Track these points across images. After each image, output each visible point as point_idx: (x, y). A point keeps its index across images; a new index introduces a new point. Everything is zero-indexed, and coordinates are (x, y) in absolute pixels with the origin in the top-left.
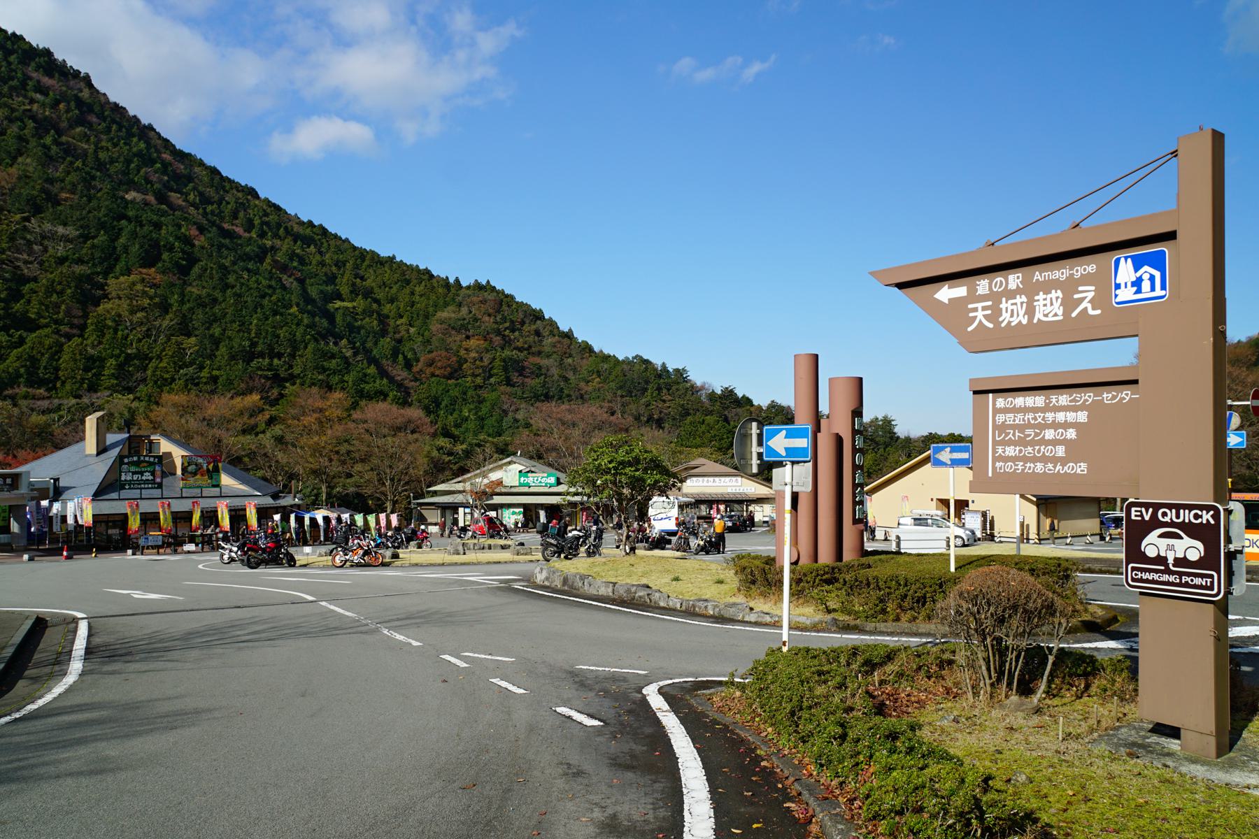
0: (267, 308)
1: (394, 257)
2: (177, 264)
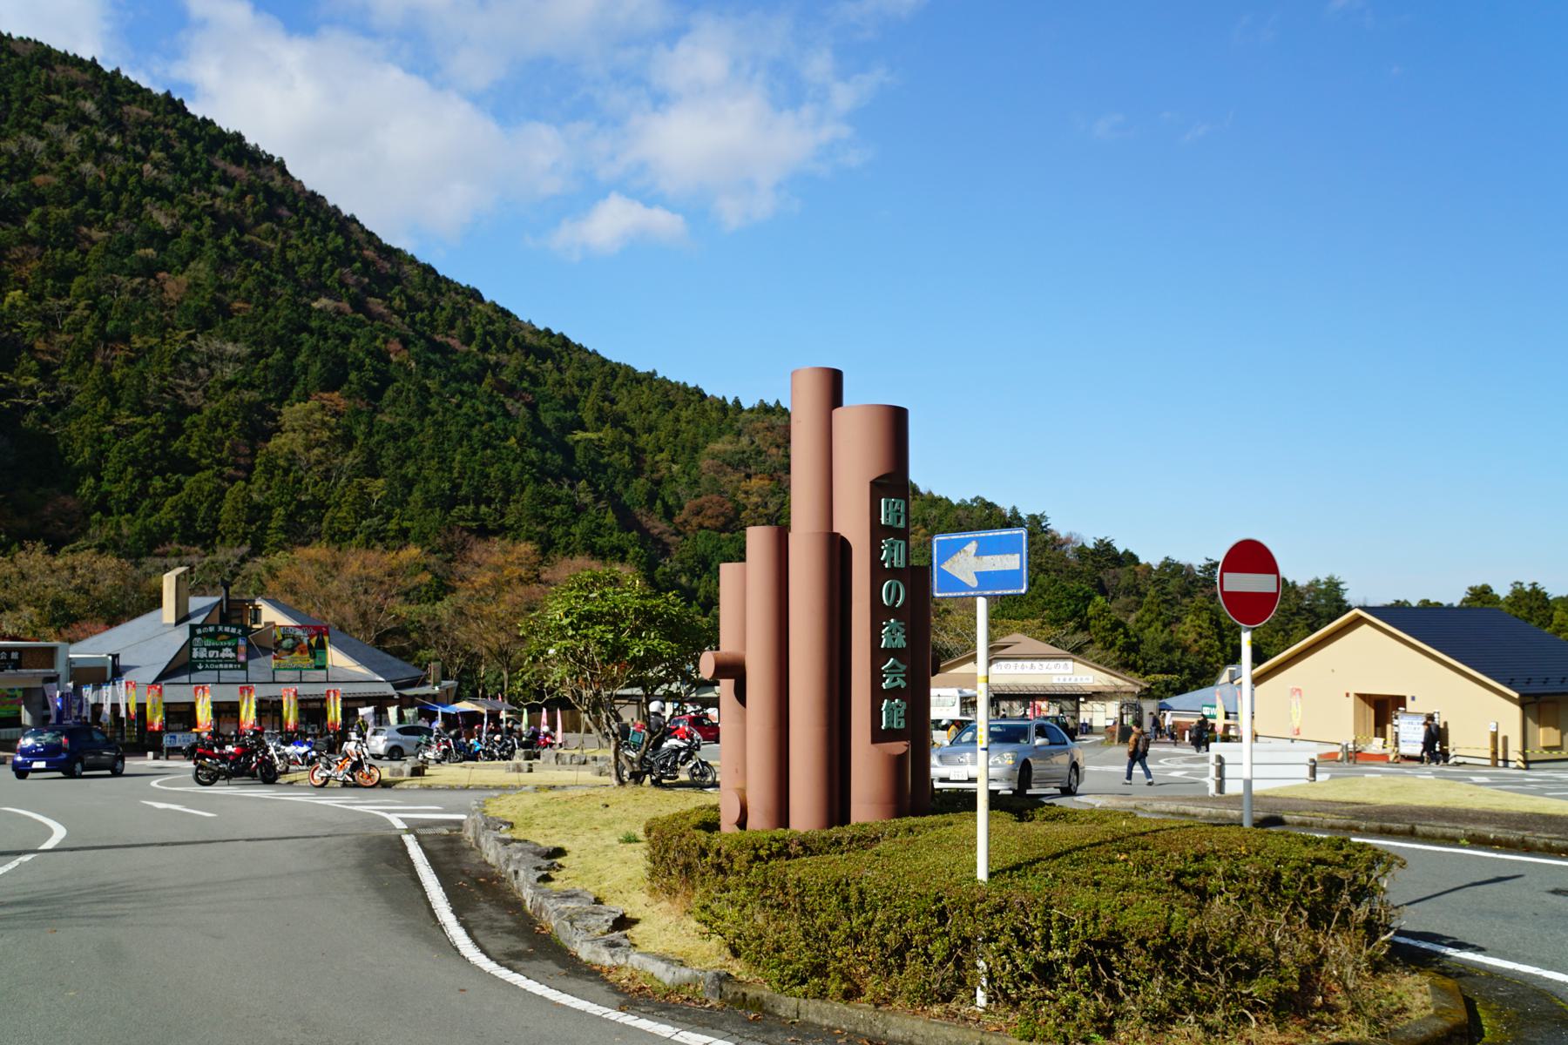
0: (475, 440)
1: (655, 373)
2: (367, 386)
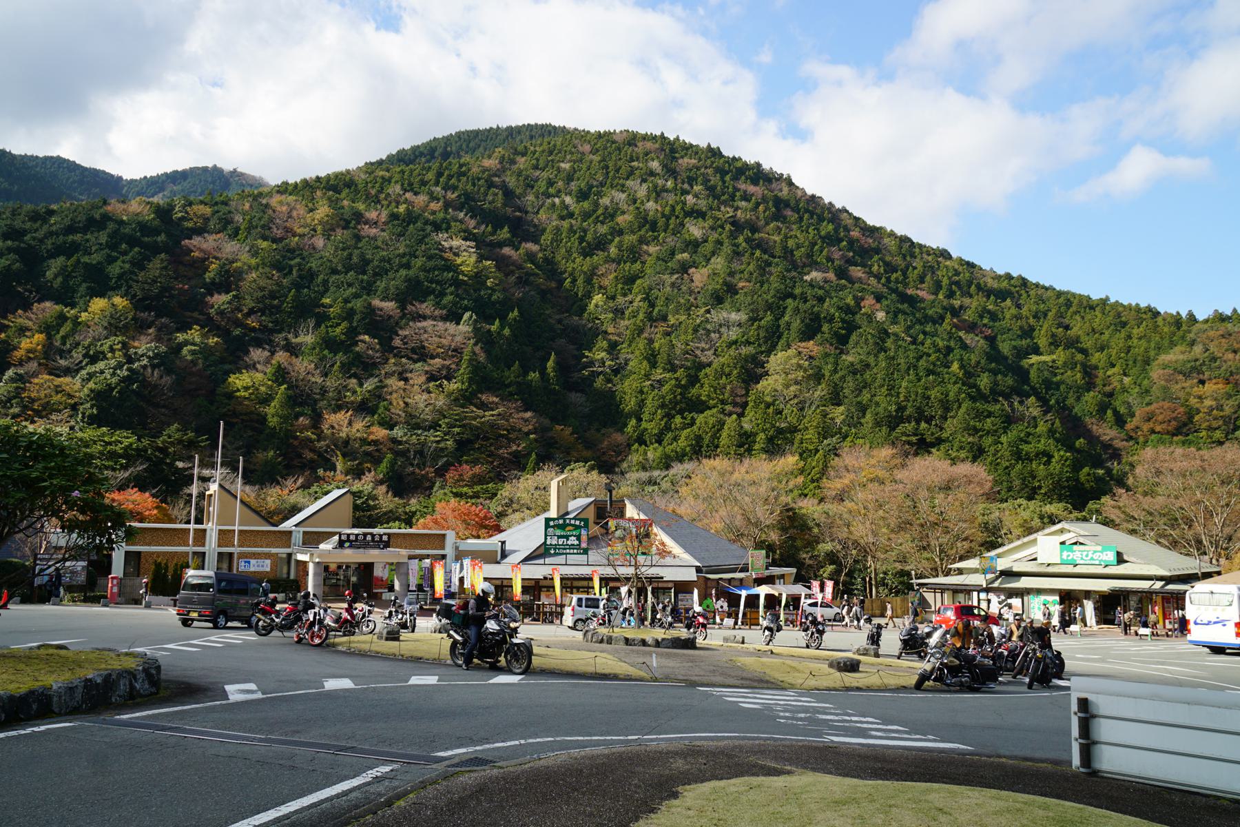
1: (1107, 299)
2: (836, 334)
